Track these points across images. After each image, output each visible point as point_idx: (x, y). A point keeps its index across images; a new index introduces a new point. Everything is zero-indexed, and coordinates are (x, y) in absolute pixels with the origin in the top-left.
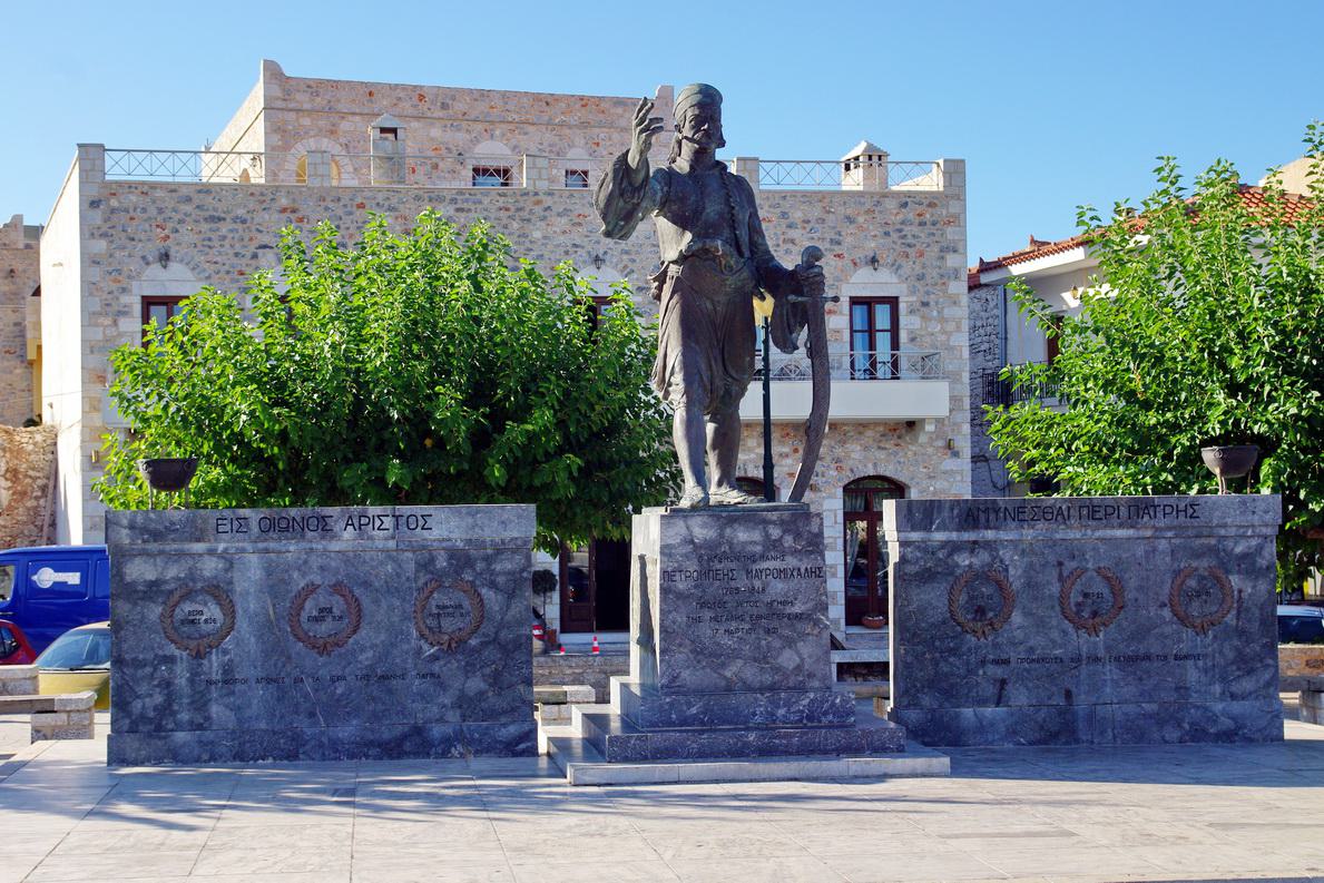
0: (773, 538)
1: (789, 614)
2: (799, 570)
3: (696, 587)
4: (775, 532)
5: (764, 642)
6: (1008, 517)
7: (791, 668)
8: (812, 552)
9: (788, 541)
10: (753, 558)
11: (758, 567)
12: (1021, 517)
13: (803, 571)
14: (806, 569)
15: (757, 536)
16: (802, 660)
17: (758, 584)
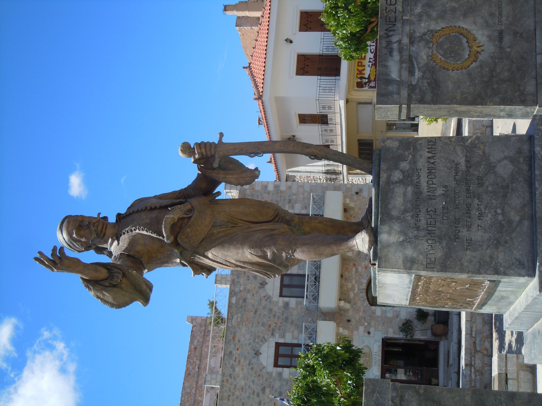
0: (401, 177)
1: (467, 167)
2: (429, 158)
3: (440, 243)
4: (397, 175)
5: (490, 189)
6: (392, 29)
7: (512, 167)
8: (415, 148)
9: (404, 165)
10: (418, 193)
11: (426, 190)
12: (393, 20)
13: (430, 155)
14: (428, 152)
15: (399, 190)
16: (506, 158)
17: (440, 191)
